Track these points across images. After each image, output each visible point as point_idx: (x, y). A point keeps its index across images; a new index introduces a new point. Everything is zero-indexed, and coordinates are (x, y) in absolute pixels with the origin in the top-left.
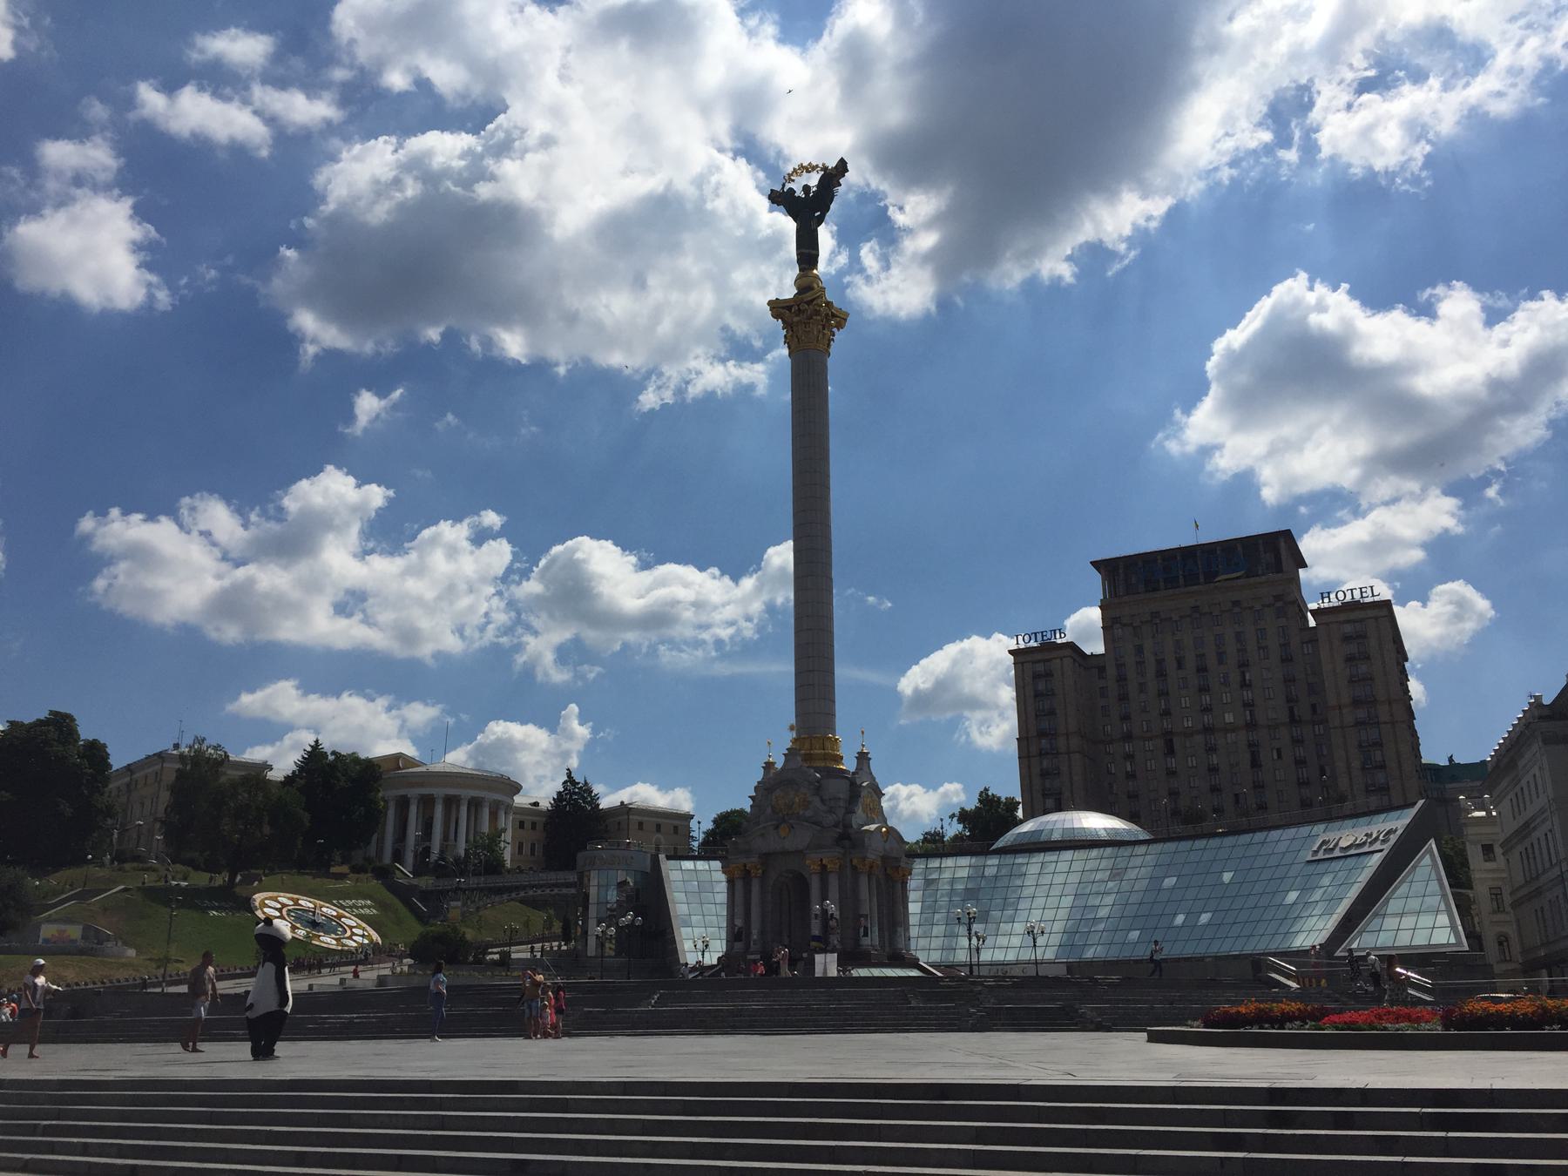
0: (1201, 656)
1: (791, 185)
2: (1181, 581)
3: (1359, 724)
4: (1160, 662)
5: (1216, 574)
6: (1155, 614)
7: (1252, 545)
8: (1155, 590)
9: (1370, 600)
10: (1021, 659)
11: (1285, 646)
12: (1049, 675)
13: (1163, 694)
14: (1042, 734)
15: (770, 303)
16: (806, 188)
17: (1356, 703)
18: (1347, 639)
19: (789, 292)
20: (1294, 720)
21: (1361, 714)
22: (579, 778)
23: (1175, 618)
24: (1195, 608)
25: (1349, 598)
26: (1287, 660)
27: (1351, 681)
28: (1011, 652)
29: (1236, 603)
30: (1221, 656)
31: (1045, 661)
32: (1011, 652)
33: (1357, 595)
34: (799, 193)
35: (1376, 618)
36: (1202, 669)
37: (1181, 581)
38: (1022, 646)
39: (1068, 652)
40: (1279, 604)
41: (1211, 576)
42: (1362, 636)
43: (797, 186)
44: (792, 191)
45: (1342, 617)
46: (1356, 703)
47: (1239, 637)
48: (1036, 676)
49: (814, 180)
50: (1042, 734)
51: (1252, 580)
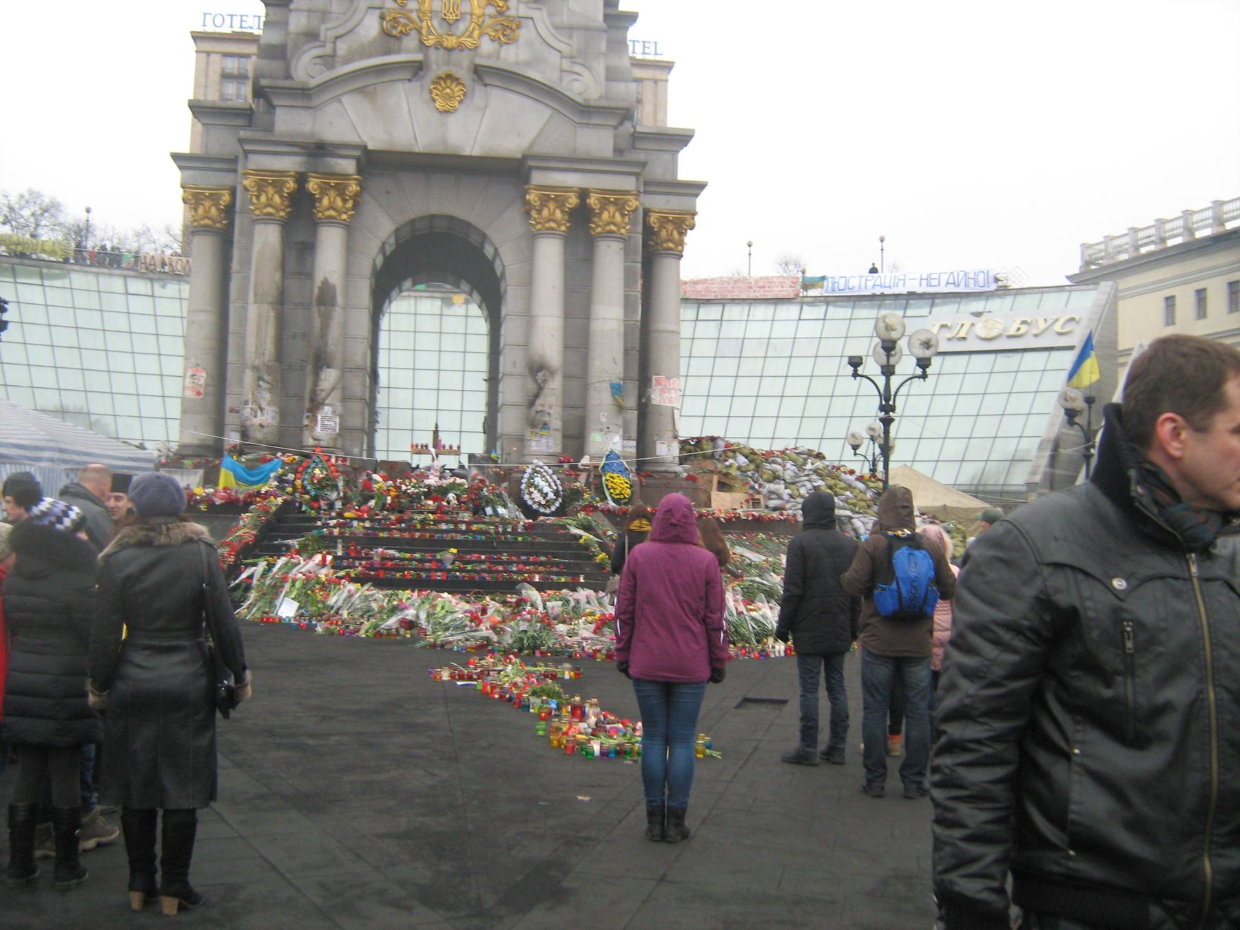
10: (207, 46)
28: (197, 37)
32: (197, 37)
38: (210, 29)
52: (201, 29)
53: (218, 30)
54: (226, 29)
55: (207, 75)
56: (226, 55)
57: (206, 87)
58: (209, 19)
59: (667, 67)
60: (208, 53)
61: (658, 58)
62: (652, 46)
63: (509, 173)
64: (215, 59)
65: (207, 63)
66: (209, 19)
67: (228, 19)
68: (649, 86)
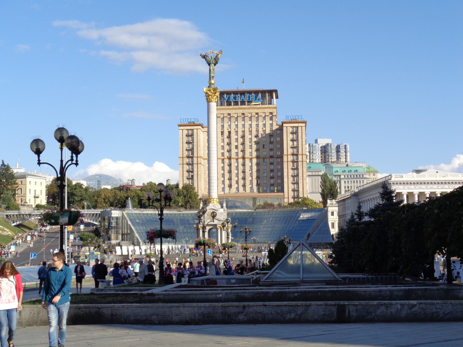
0: (244, 132)
3: (293, 162)
6: (229, 114)
7: (263, 92)
9: (300, 120)
17: (293, 155)
18: (292, 133)
22: (6, 163)
29: (257, 114)
30: (251, 131)
31: (190, 130)
33: (297, 118)
36: (243, 137)
38: (183, 123)
39: (200, 127)
40: (271, 116)
41: (249, 102)
45: (292, 125)
47: (257, 125)
49: (214, 56)
50: (188, 157)
51: (263, 106)
53: (185, 123)
56: (187, 130)
63: (216, 225)
68: (300, 129)
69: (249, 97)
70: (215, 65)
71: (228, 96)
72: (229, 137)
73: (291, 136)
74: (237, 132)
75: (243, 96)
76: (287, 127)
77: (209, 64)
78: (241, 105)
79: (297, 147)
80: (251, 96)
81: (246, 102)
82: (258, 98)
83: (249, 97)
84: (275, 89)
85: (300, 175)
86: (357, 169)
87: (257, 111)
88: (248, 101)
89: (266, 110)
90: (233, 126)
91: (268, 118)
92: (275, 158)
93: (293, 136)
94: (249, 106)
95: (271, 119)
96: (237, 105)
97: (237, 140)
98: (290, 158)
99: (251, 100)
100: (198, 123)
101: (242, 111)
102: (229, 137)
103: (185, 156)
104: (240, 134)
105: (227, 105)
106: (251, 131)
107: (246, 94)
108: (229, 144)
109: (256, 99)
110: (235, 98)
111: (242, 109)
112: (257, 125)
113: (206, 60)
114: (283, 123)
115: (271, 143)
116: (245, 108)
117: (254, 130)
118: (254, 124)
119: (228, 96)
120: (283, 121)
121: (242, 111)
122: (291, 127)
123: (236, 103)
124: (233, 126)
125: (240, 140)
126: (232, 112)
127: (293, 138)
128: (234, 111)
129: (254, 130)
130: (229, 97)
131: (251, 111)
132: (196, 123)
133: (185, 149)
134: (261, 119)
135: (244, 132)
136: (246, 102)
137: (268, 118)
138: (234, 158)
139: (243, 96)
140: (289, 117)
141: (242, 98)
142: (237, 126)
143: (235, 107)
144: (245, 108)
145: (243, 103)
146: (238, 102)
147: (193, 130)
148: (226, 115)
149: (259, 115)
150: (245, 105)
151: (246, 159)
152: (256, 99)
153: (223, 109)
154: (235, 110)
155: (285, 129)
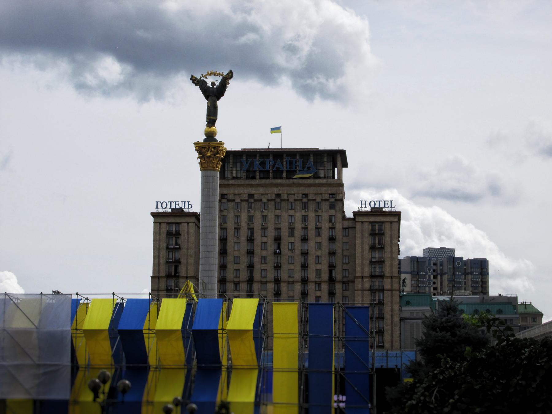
0: (278, 229)
1: (206, 80)
2: (271, 174)
4: (251, 230)
5: (294, 172)
6: (251, 196)
8: (254, 178)
9: (387, 210)
10: (159, 220)
11: (332, 228)
12: (178, 234)
13: (250, 253)
14: (169, 276)
15: (195, 144)
16: (213, 84)
17: (372, 277)
19: (201, 138)
20: (332, 280)
21: (377, 283)
23: (265, 200)
24: (278, 195)
25: (377, 206)
26: (332, 239)
27: (371, 262)
28: (154, 215)
29: (306, 195)
30: (292, 231)
31: (176, 223)
32: (154, 215)
33: (382, 205)
34: (209, 85)
35: (391, 222)
36: (278, 239)
37: (271, 174)
38: (160, 211)
40: (332, 200)
41: (291, 174)
42: (381, 234)
43: (209, 81)
44: (206, 83)
45: (372, 219)
46: (372, 277)
47: (305, 219)
48: (169, 234)
49: (218, 80)
50: (169, 276)
51: (317, 181)
52: (155, 211)
54: (168, 210)
55: (160, 234)
56: (168, 223)
57: (159, 240)
58: (159, 204)
59: (398, 215)
60: (160, 223)
61: (393, 210)
62: (389, 203)
64: (164, 226)
65: (160, 228)
66: (159, 204)
67: (169, 204)
68: (387, 226)
69: (291, 163)
70: (218, 100)
71: (250, 160)
72: (251, 240)
73: (368, 241)
74: (264, 229)
75: (279, 161)
76: (362, 222)
77: (207, 97)
78: (274, 178)
79: (381, 262)
80: (294, 160)
81: (284, 175)
82: (308, 165)
83: (291, 163)
84: (341, 148)
85: (387, 317)
86: (500, 307)
87: (306, 190)
88: (287, 172)
89: (323, 190)
90: (258, 219)
91: (325, 205)
92: (339, 282)
93: (374, 239)
94: (291, 181)
95: (332, 206)
96: (268, 178)
97: (264, 246)
98: (367, 284)
99: (294, 169)
100: (191, 211)
101: (276, 190)
102: (251, 240)
103: (163, 274)
104: (271, 234)
105: (247, 178)
106: (292, 231)
107: (285, 157)
108: (250, 253)
109: (303, 168)
110: (263, 164)
111: (276, 185)
112: (305, 219)
113: (201, 89)
114: (354, 213)
115: (332, 253)
116: (282, 185)
117: (298, 227)
118: (298, 215)
119: (250, 160)
120: (356, 210)
121: (276, 190)
122: (370, 222)
123: (265, 175)
124: (258, 219)
125: (272, 246)
126: (257, 191)
127: (374, 243)
128: (261, 190)
129: (298, 227)
130: (252, 164)
131: (294, 190)
132: (186, 210)
133: (163, 262)
134: (312, 206)
135: (278, 229)
136: (284, 175)
137: (325, 205)
138: (258, 282)
139: (279, 161)
140: (368, 203)
141: (276, 166)
142: (264, 218)
143: (263, 181)
144: (282, 185)
145: (278, 174)
146: (269, 171)
147: (179, 224)
148: (246, 197)
149: (311, 197)
150: (282, 178)
151: (282, 285)
152: (303, 168)
153: (239, 186)
154: (263, 189)
155: (358, 226)
